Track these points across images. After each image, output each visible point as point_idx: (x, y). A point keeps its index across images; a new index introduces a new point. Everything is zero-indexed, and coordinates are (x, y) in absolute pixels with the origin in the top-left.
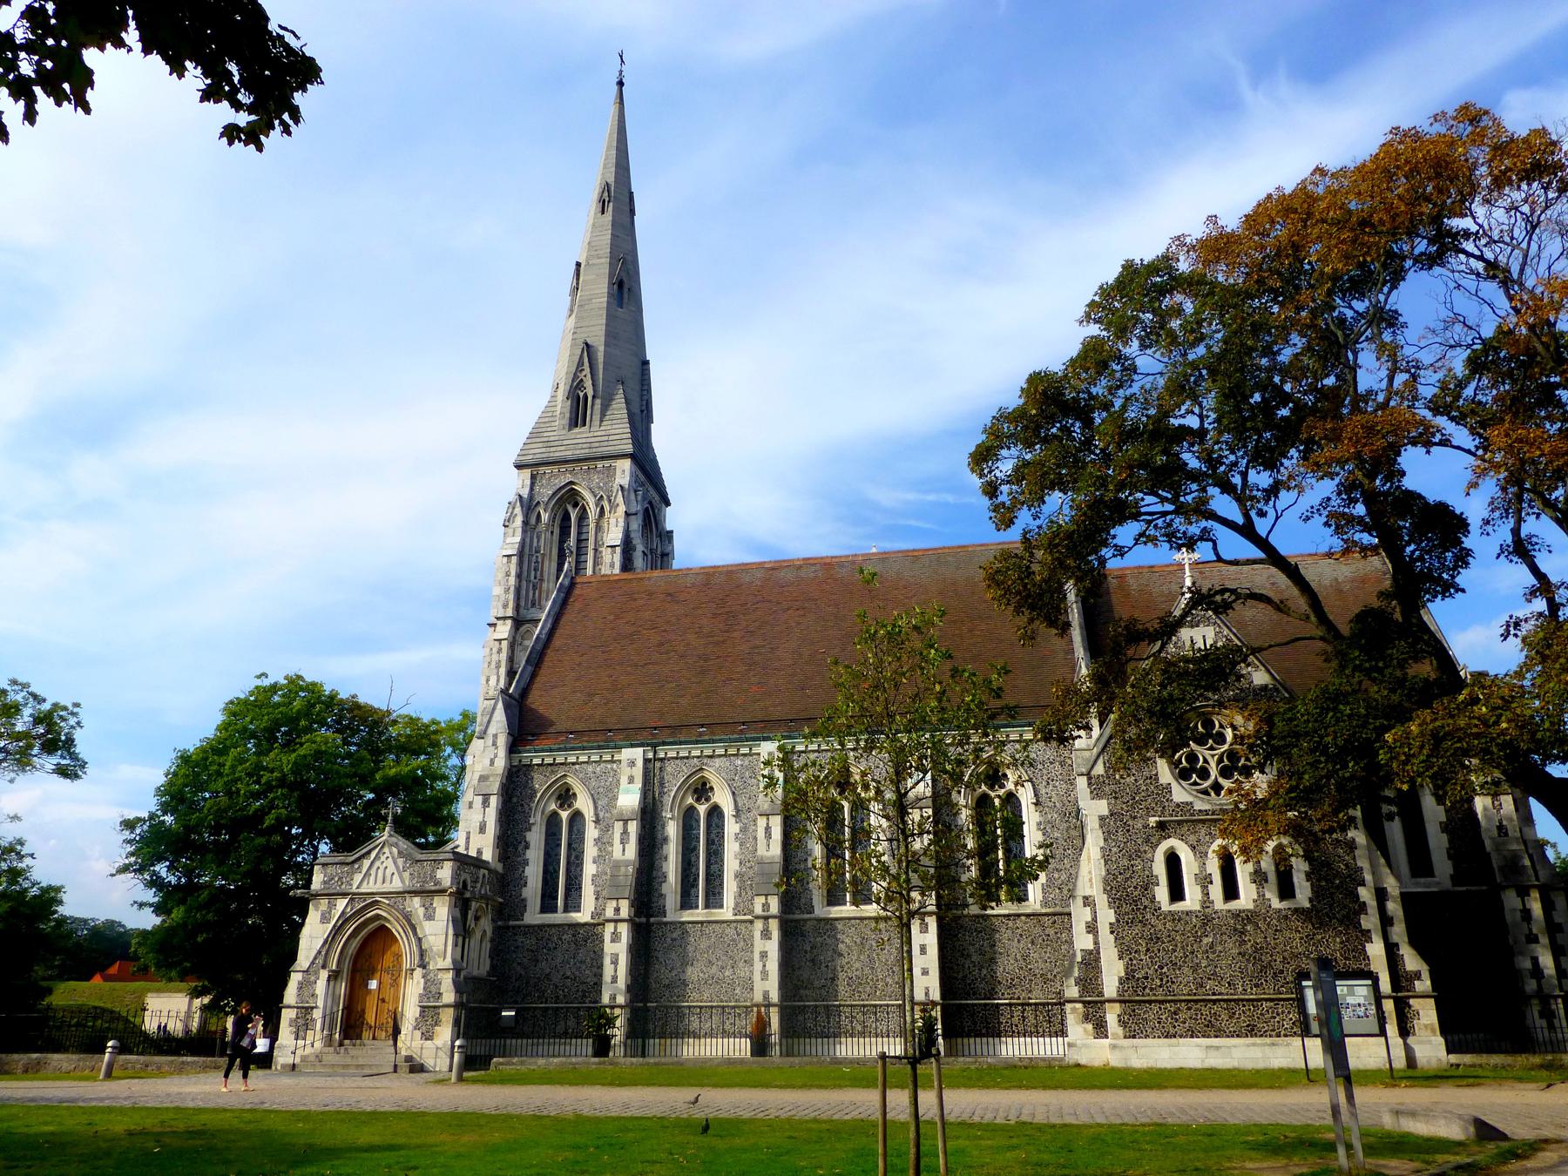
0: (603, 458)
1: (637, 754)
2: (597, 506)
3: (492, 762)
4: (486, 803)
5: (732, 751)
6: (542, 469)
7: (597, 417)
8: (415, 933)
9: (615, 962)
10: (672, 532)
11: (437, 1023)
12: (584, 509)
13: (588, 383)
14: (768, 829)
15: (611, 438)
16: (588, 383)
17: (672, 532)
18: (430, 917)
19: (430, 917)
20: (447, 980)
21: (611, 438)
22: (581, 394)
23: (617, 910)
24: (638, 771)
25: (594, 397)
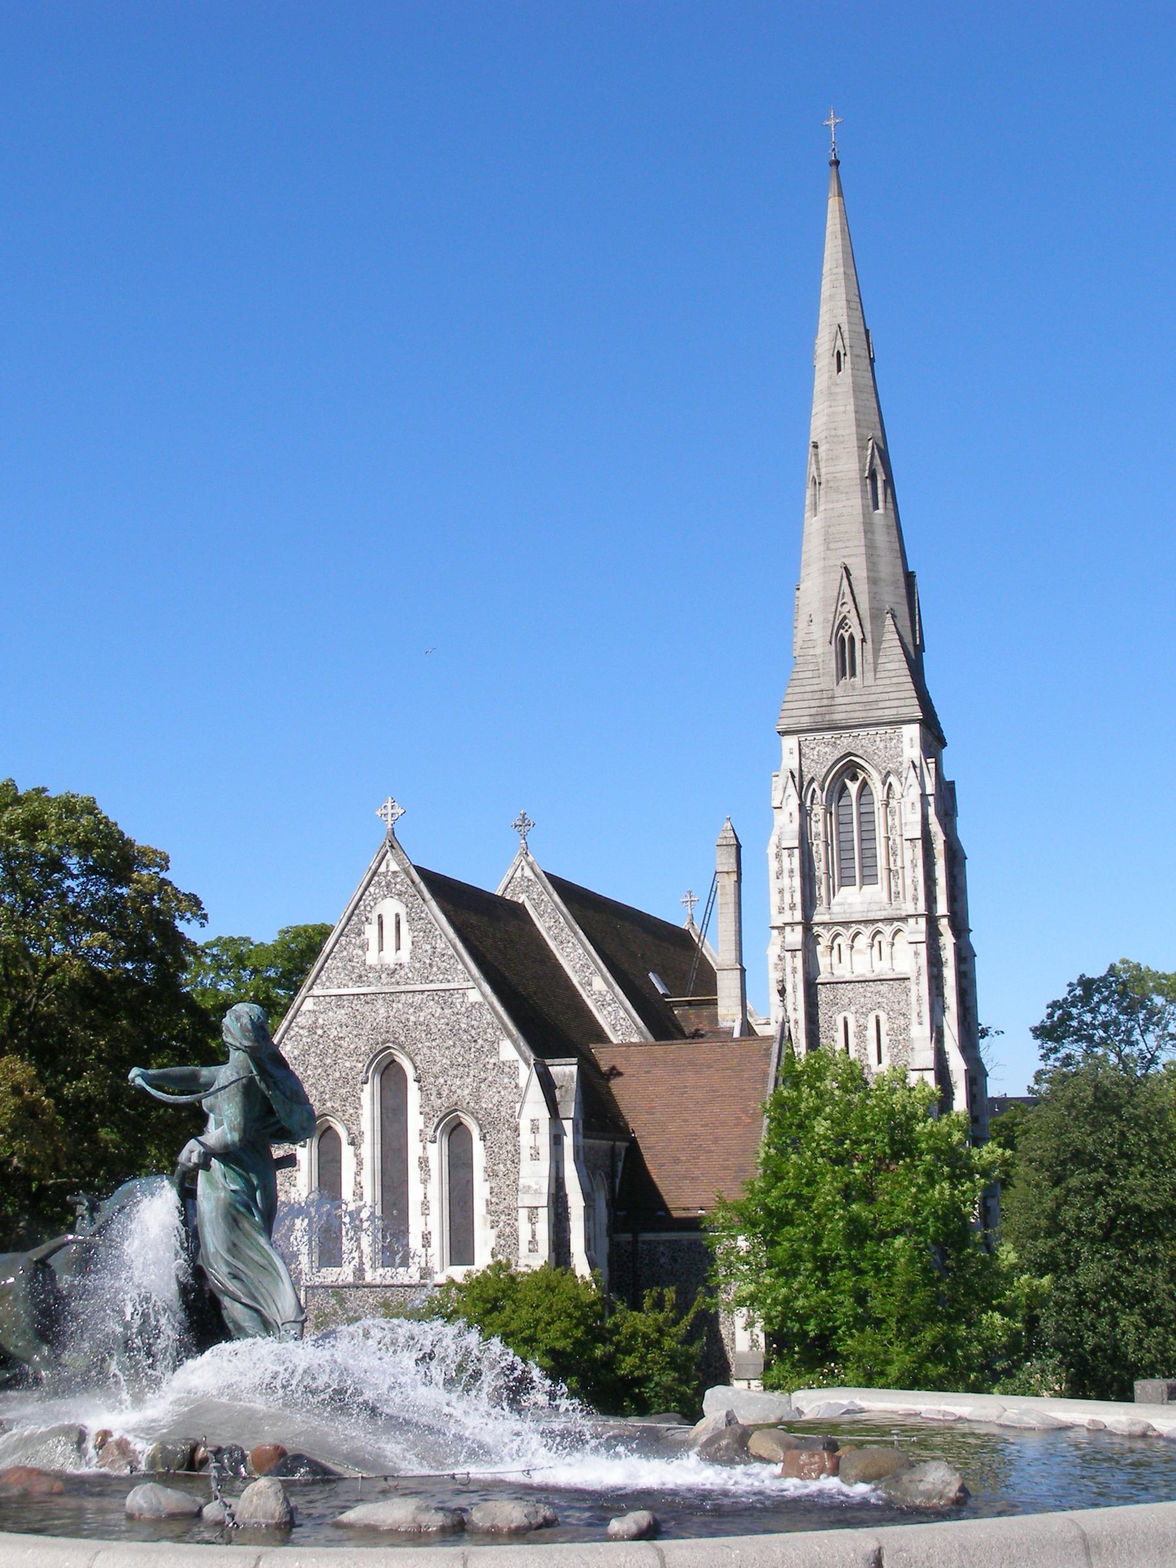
2: (884, 784)
7: (869, 667)
10: (953, 783)
12: (864, 784)
13: (853, 620)
16: (853, 620)
17: (953, 783)
22: (846, 636)
25: (863, 640)
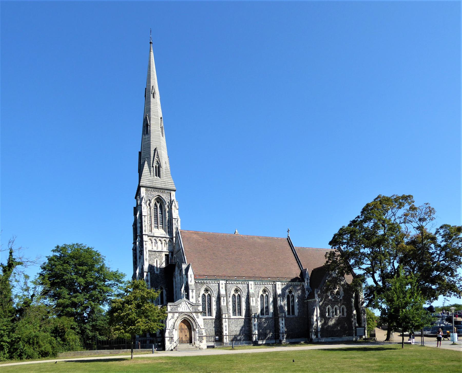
0: (167, 190)
1: (224, 282)
3: (191, 282)
4: (192, 291)
5: (243, 283)
6: (148, 189)
8: (195, 322)
9: (226, 327)
11: (203, 339)
14: (253, 300)
15: (169, 183)
18: (198, 318)
19: (198, 318)
20: (203, 331)
21: (169, 183)
23: (225, 316)
24: (224, 286)
